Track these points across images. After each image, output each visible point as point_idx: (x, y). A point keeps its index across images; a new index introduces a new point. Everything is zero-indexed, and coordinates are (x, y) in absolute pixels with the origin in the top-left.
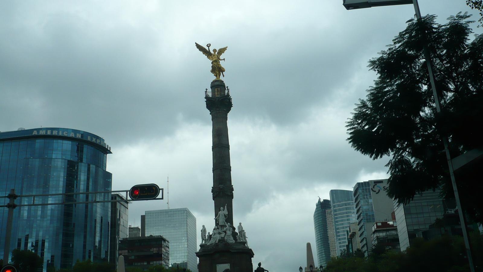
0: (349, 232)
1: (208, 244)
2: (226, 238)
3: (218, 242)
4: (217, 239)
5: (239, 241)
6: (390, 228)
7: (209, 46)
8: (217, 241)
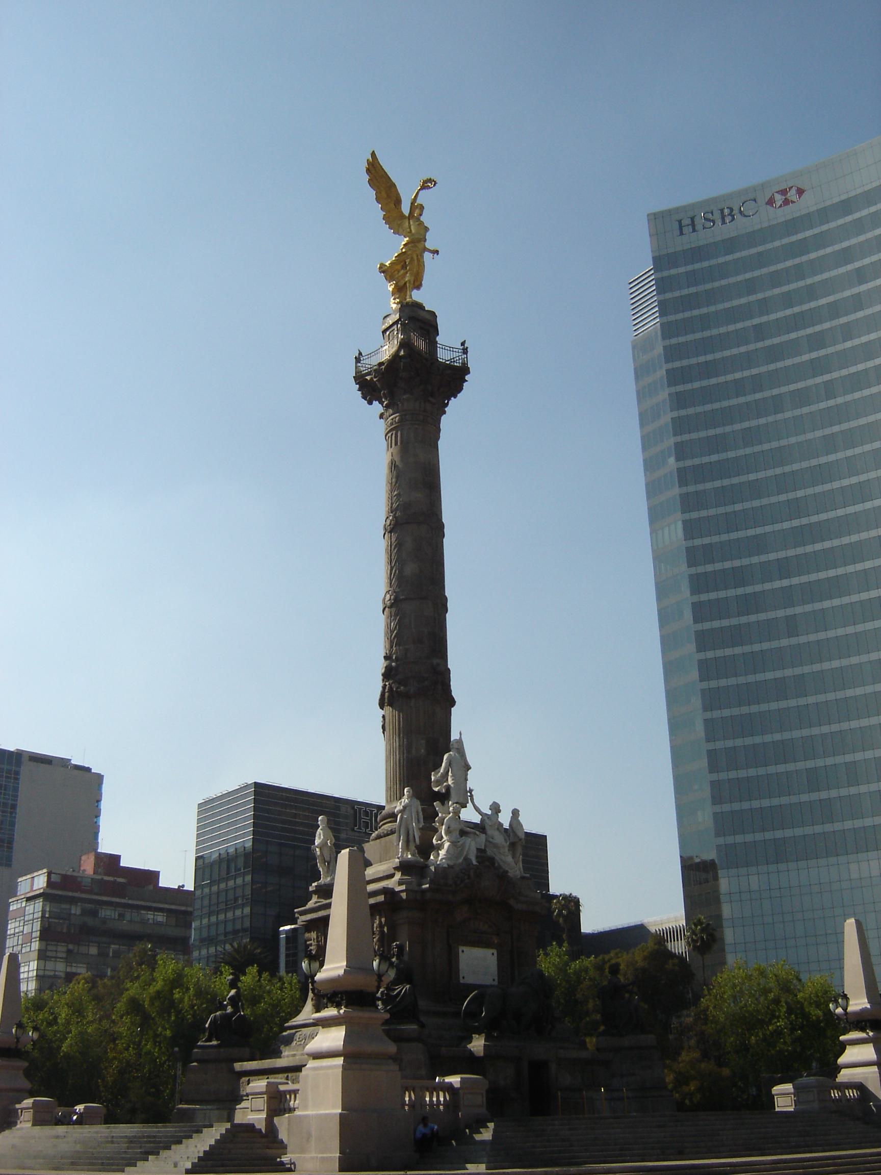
2: (489, 852)
6: (76, 895)
7: (427, 184)
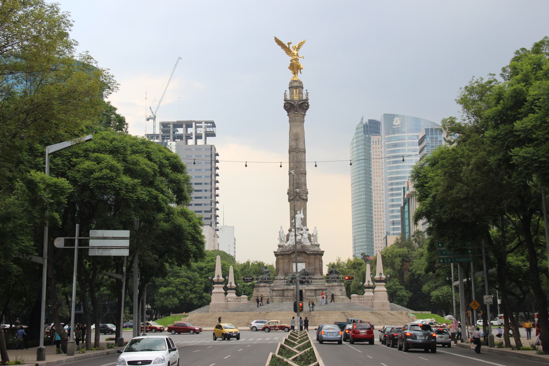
0: (406, 189)
1: (286, 244)
2: (302, 240)
5: (313, 243)
7: (289, 44)
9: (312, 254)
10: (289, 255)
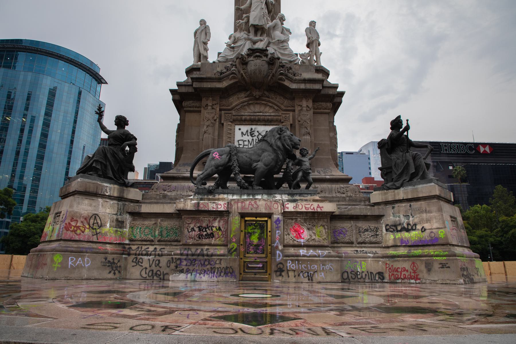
3: (249, 55)
4: (242, 50)
8: (244, 52)
9: (305, 94)
10: (224, 94)
